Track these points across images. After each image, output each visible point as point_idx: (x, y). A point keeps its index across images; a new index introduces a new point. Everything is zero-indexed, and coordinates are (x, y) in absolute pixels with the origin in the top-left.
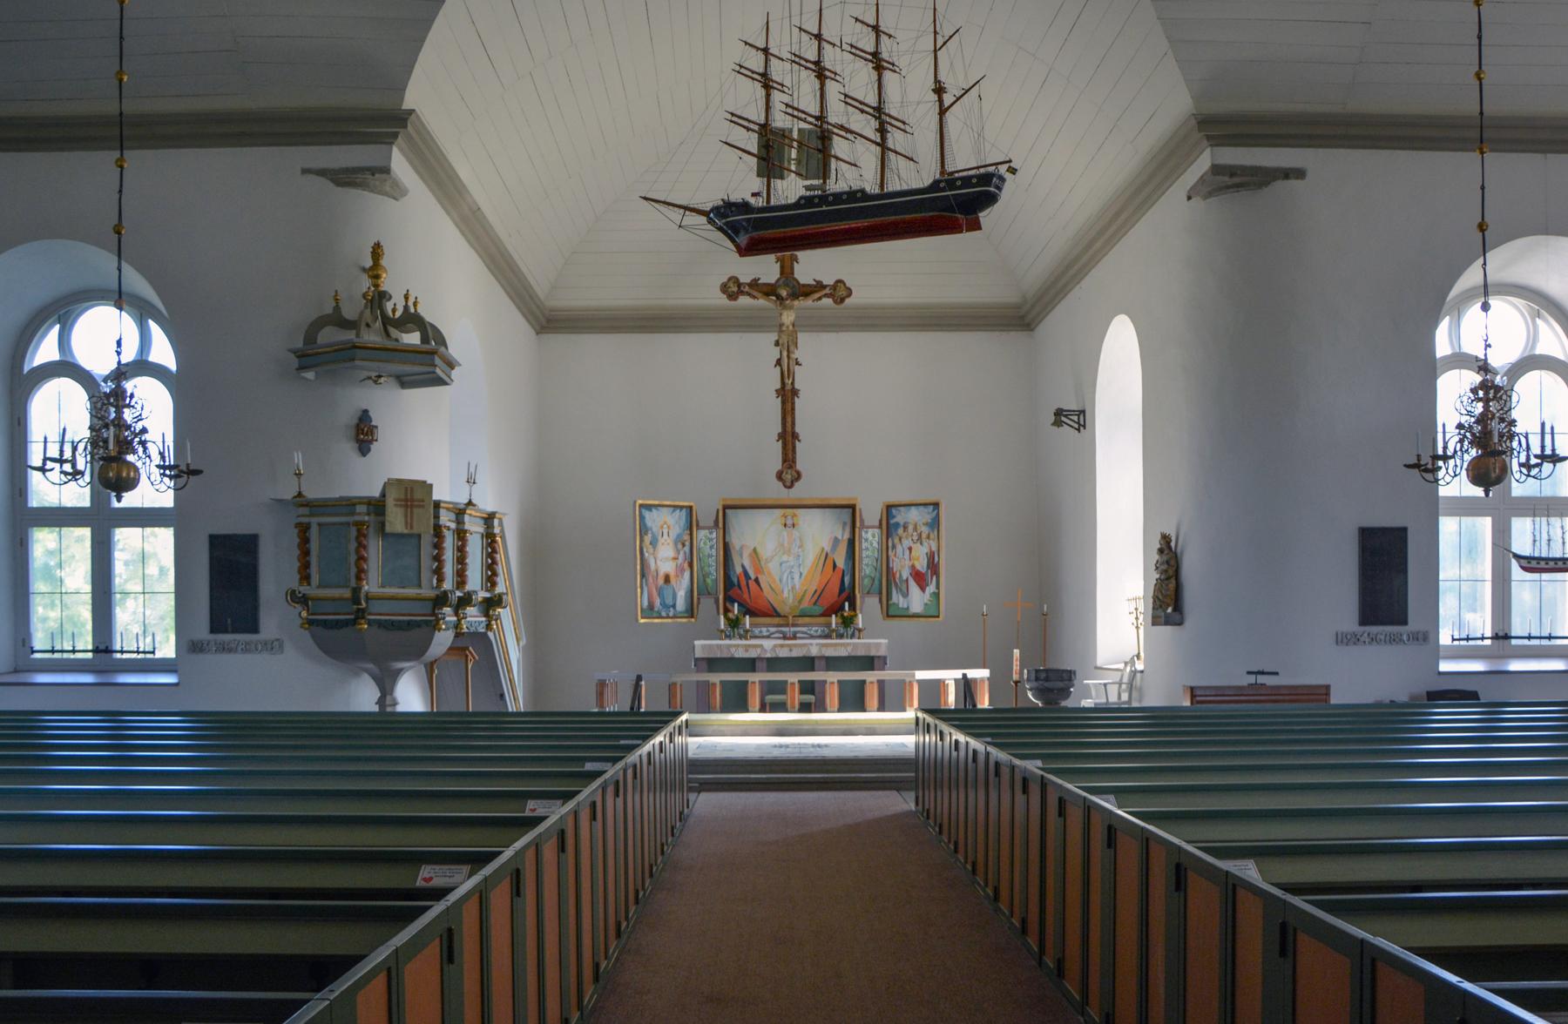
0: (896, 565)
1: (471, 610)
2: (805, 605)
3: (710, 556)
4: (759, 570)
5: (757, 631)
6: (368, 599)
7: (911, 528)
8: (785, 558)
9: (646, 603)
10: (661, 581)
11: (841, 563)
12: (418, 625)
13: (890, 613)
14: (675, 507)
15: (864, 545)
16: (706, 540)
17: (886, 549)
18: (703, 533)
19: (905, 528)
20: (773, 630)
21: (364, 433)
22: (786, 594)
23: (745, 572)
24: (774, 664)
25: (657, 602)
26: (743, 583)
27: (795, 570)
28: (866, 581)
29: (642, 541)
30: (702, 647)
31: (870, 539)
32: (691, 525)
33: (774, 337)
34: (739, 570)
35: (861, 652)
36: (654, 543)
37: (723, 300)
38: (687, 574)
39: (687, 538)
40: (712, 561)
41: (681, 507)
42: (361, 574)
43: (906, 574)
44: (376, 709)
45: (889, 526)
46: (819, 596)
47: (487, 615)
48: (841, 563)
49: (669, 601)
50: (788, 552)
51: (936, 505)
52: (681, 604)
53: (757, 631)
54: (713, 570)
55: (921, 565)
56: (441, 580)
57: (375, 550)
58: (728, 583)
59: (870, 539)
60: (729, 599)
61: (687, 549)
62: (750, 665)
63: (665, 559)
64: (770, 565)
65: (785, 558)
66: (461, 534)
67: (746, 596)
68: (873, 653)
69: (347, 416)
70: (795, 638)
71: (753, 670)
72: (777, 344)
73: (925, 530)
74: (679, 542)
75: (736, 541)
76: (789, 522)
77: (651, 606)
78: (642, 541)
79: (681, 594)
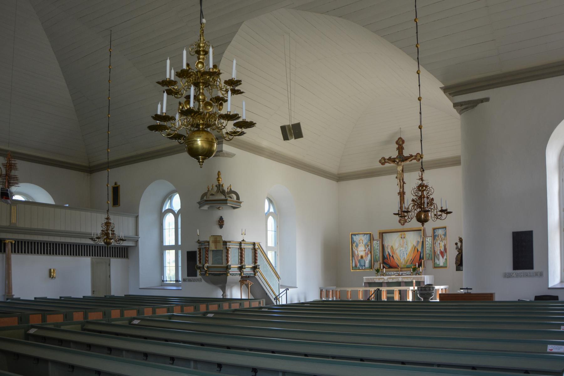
0: (436, 250)
1: (244, 270)
2: (408, 264)
4: (393, 253)
6: (208, 267)
8: (401, 249)
9: (354, 265)
10: (360, 258)
11: (420, 250)
12: (222, 274)
14: (365, 234)
16: (376, 244)
17: (434, 244)
18: (375, 242)
21: (221, 222)
23: (389, 254)
24: (389, 284)
25: (358, 265)
26: (388, 257)
27: (405, 252)
28: (428, 255)
29: (352, 245)
30: (365, 279)
31: (429, 240)
32: (371, 238)
33: (396, 175)
34: (387, 253)
36: (357, 246)
37: (380, 166)
38: (369, 255)
39: (369, 244)
40: (378, 251)
41: (367, 234)
42: (207, 261)
43: (438, 252)
44: (222, 297)
45: (434, 237)
46: (413, 261)
47: (254, 271)
48: (420, 250)
49: (363, 264)
50: (402, 246)
51: (445, 228)
52: (367, 264)
55: (442, 249)
56: (228, 262)
57: (210, 255)
58: (384, 258)
59: (429, 240)
60: (384, 263)
61: (369, 247)
62: (381, 284)
63: (361, 250)
65: (401, 249)
66: (241, 249)
69: (217, 218)
71: (382, 286)
72: (396, 178)
73: (443, 237)
74: (366, 245)
75: (386, 244)
76: (403, 237)
77: (356, 266)
78: (352, 245)
79: (367, 263)
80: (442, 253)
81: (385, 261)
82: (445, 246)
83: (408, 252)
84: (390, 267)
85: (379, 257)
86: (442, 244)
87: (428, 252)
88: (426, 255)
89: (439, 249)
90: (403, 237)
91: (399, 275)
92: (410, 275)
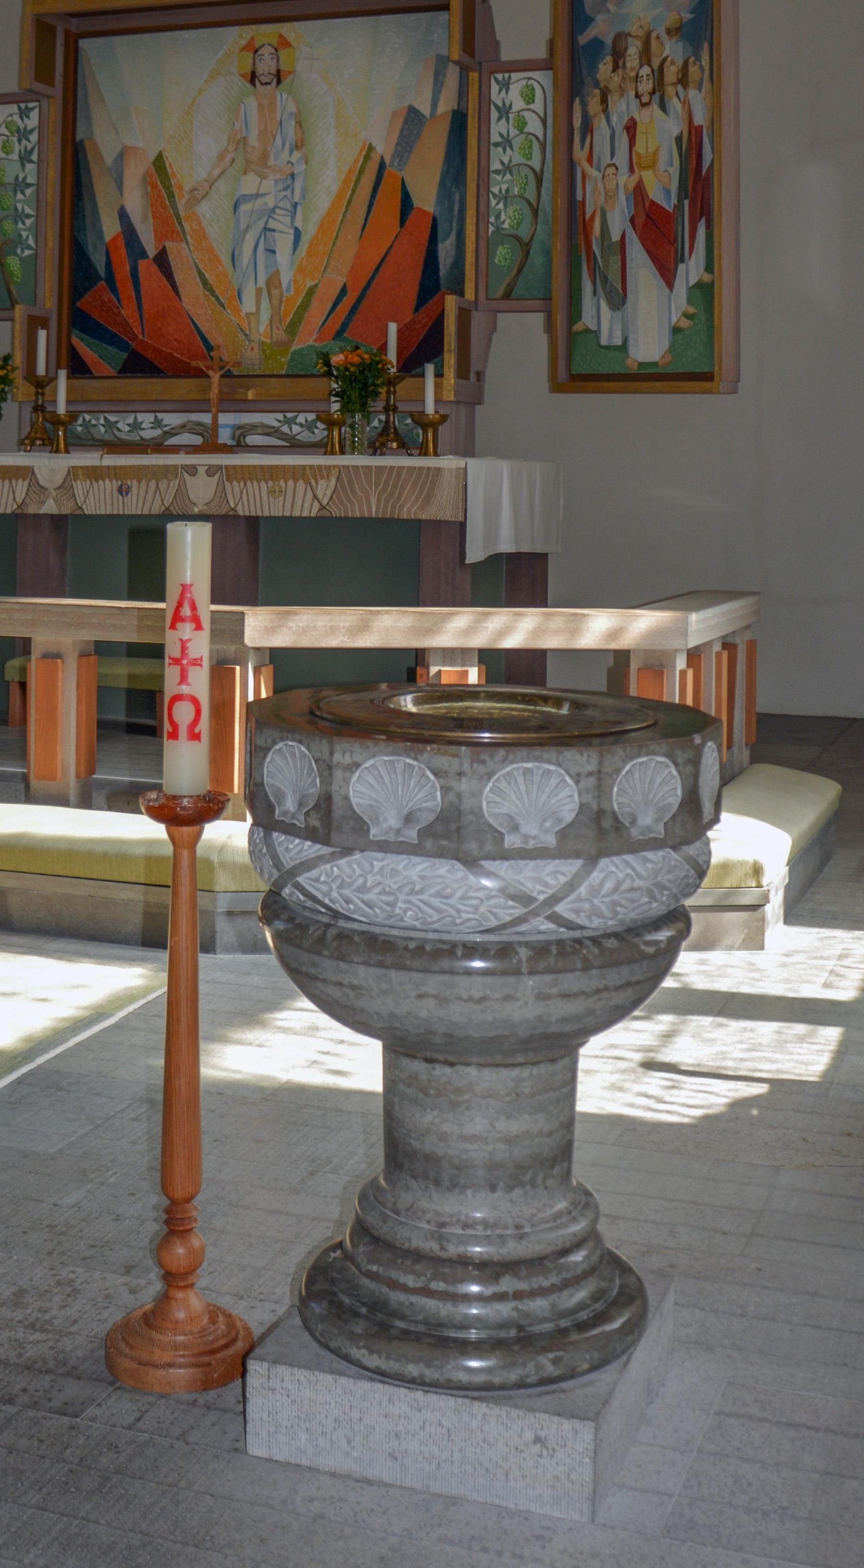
0: (592, 196)
2: (308, 339)
3: (20, 185)
4: (169, 223)
5: (99, 424)
7: (633, 50)
11: (426, 198)
13: (583, 370)
15: (498, 128)
17: (570, 132)
19: (618, 55)
20: (172, 420)
22: (248, 305)
26: (123, 270)
27: (281, 223)
28: (502, 254)
31: (523, 103)
34: (111, 228)
35: (371, 505)
40: (24, 203)
43: (618, 222)
50: (259, 164)
53: (99, 424)
54: (25, 229)
55: (663, 185)
58: (80, 271)
64: (204, 209)
65: (249, 184)
67: (128, 312)
68: (409, 510)
70: (239, 446)
73: (672, 51)
75: (103, 140)
76: (267, 66)
80: (658, 231)
81: (87, 302)
82: (691, 145)
83: (309, 232)
84: (138, 364)
85: (32, 265)
86: (662, 130)
87: (507, 217)
88: (485, 246)
89: (624, 180)
90: (267, 66)
91: (211, 446)
92: (324, 447)
